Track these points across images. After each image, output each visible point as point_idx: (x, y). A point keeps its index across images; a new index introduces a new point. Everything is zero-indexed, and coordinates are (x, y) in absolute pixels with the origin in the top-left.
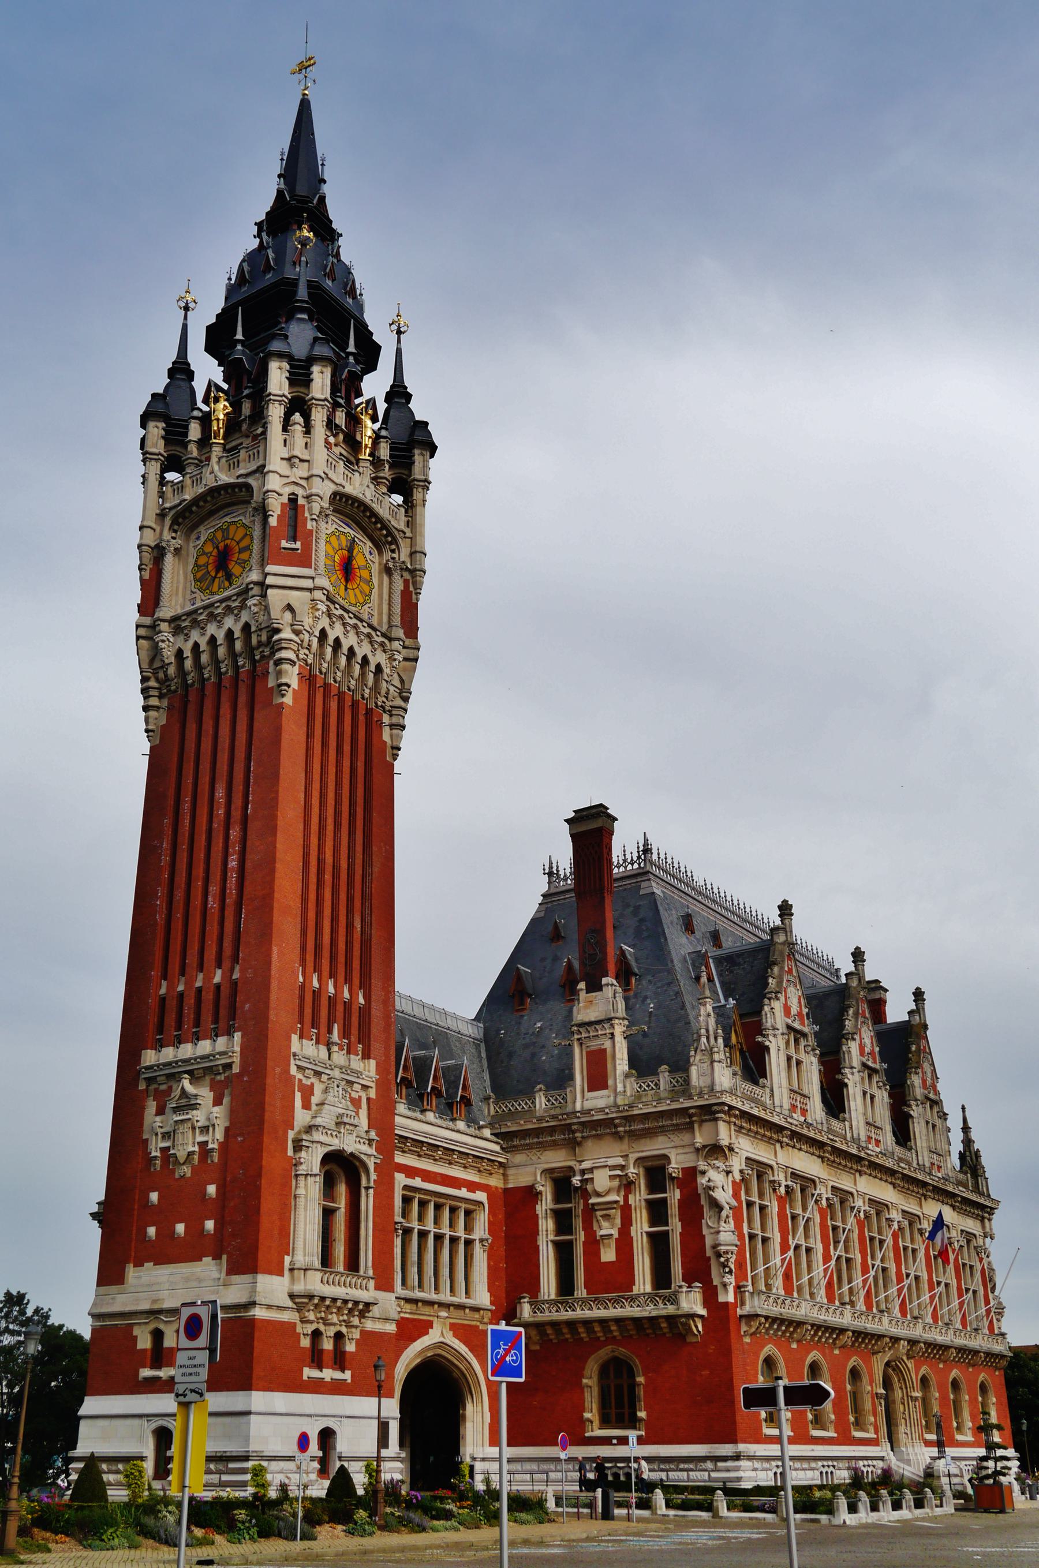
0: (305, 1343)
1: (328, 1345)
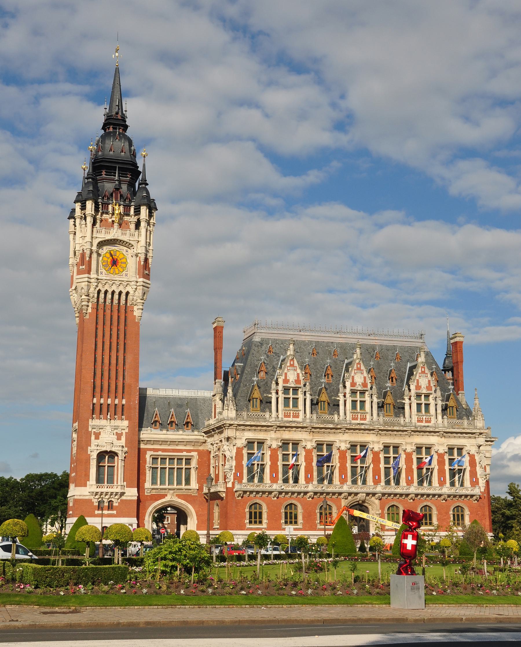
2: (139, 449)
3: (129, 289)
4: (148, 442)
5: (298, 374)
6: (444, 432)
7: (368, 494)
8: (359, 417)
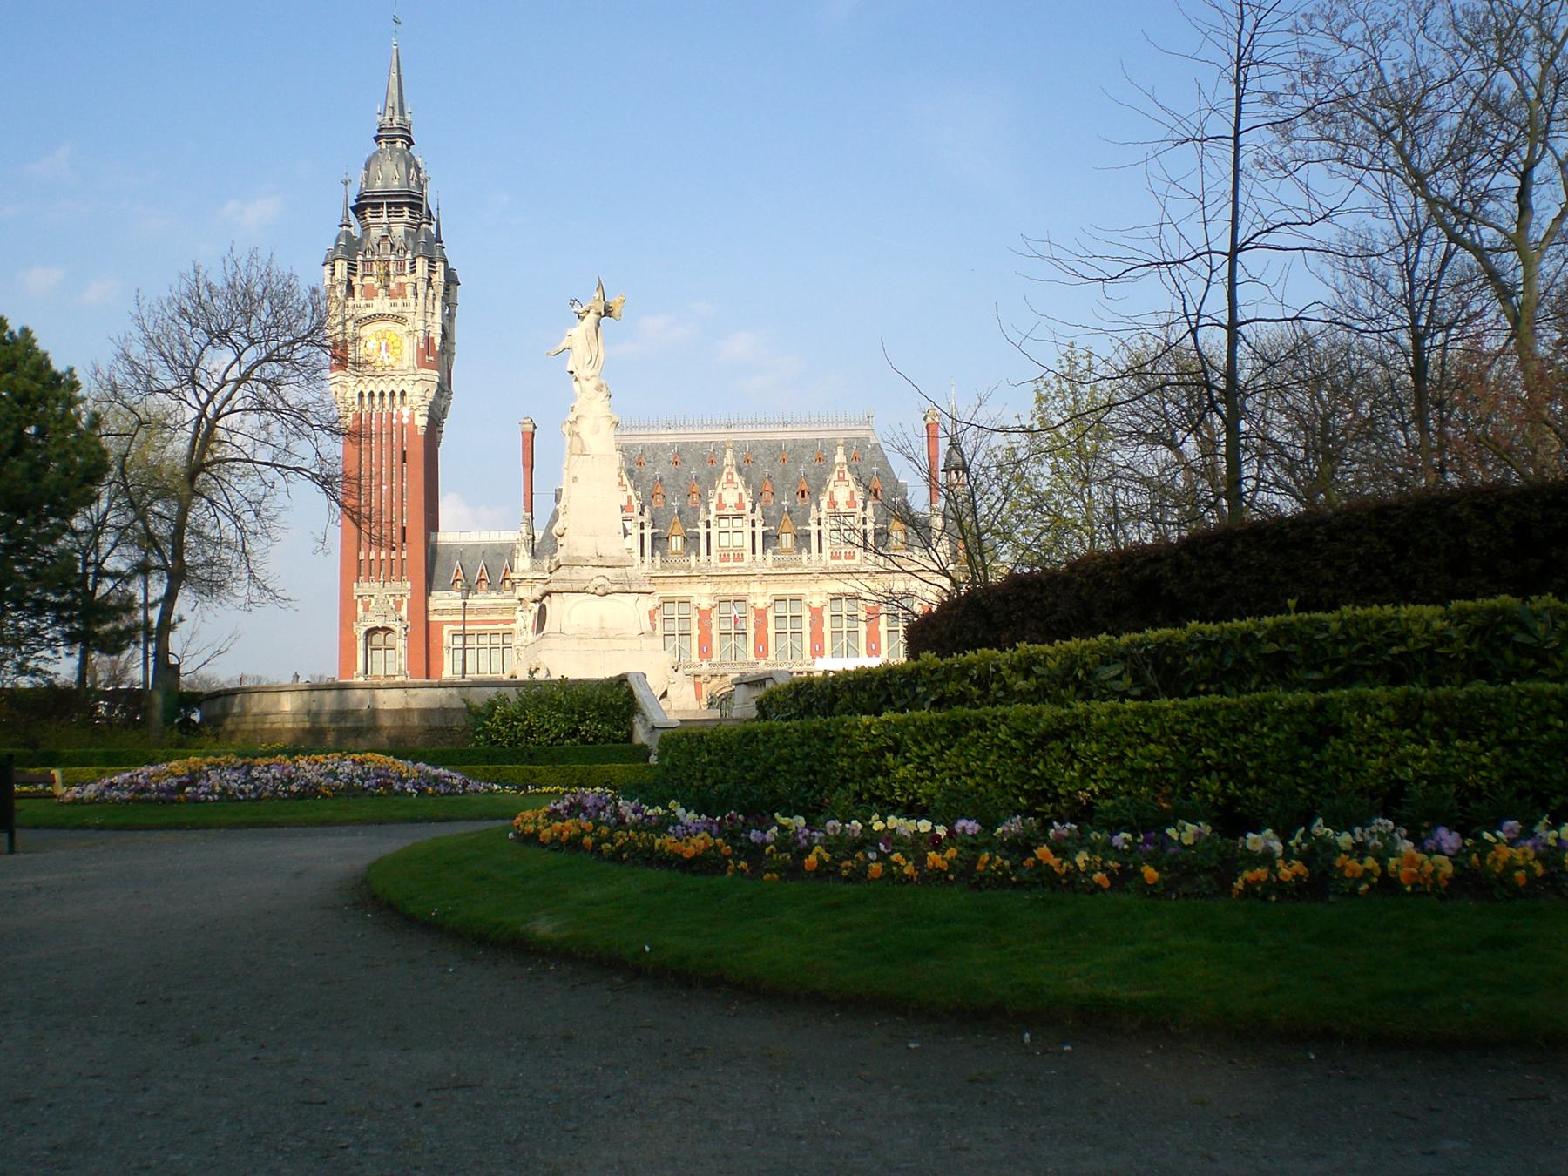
2: (428, 623)
3: (404, 386)
4: (444, 612)
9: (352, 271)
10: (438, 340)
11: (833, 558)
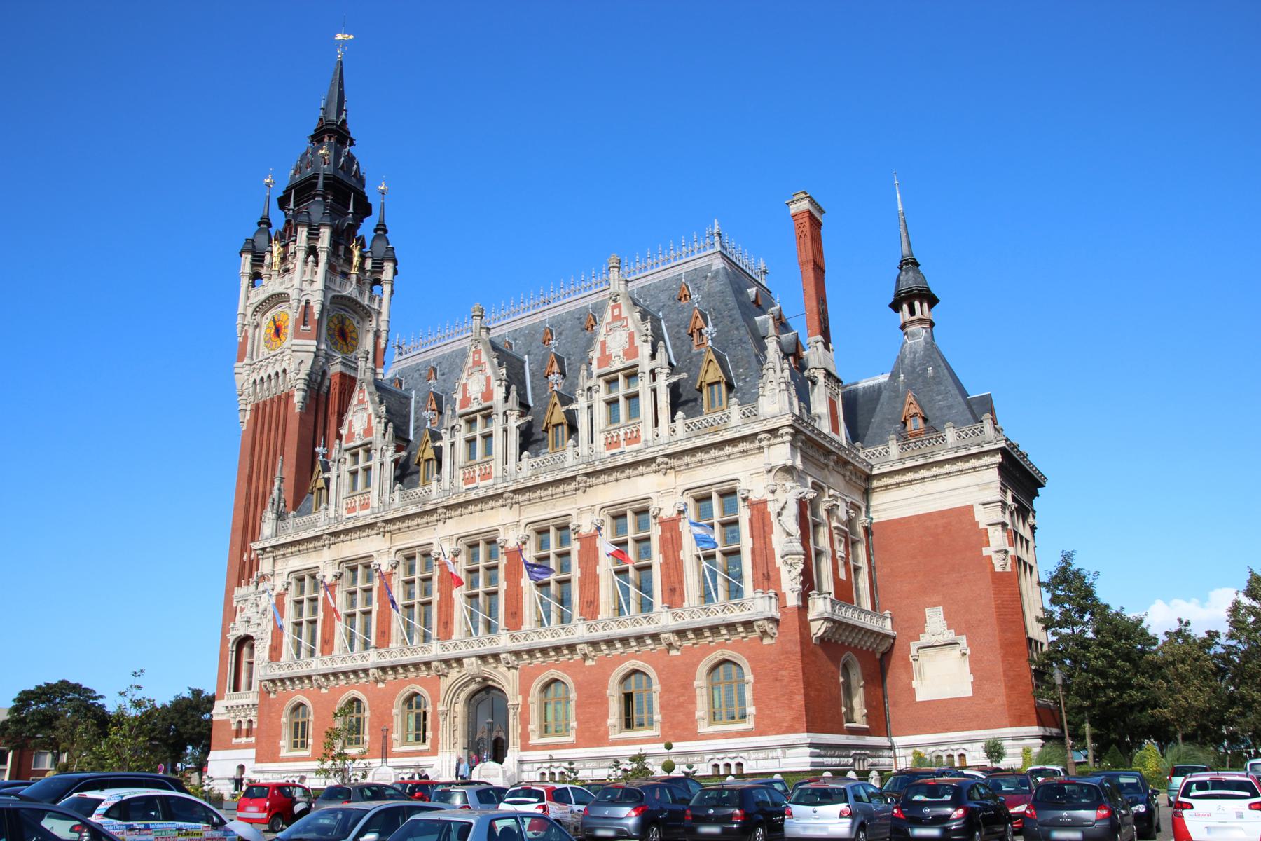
0: (234, 727)
1: (245, 727)
3: (284, 365)
5: (370, 416)
6: (669, 456)
7: (483, 658)
8: (478, 472)
9: (258, 260)
10: (317, 309)
11: (609, 445)
